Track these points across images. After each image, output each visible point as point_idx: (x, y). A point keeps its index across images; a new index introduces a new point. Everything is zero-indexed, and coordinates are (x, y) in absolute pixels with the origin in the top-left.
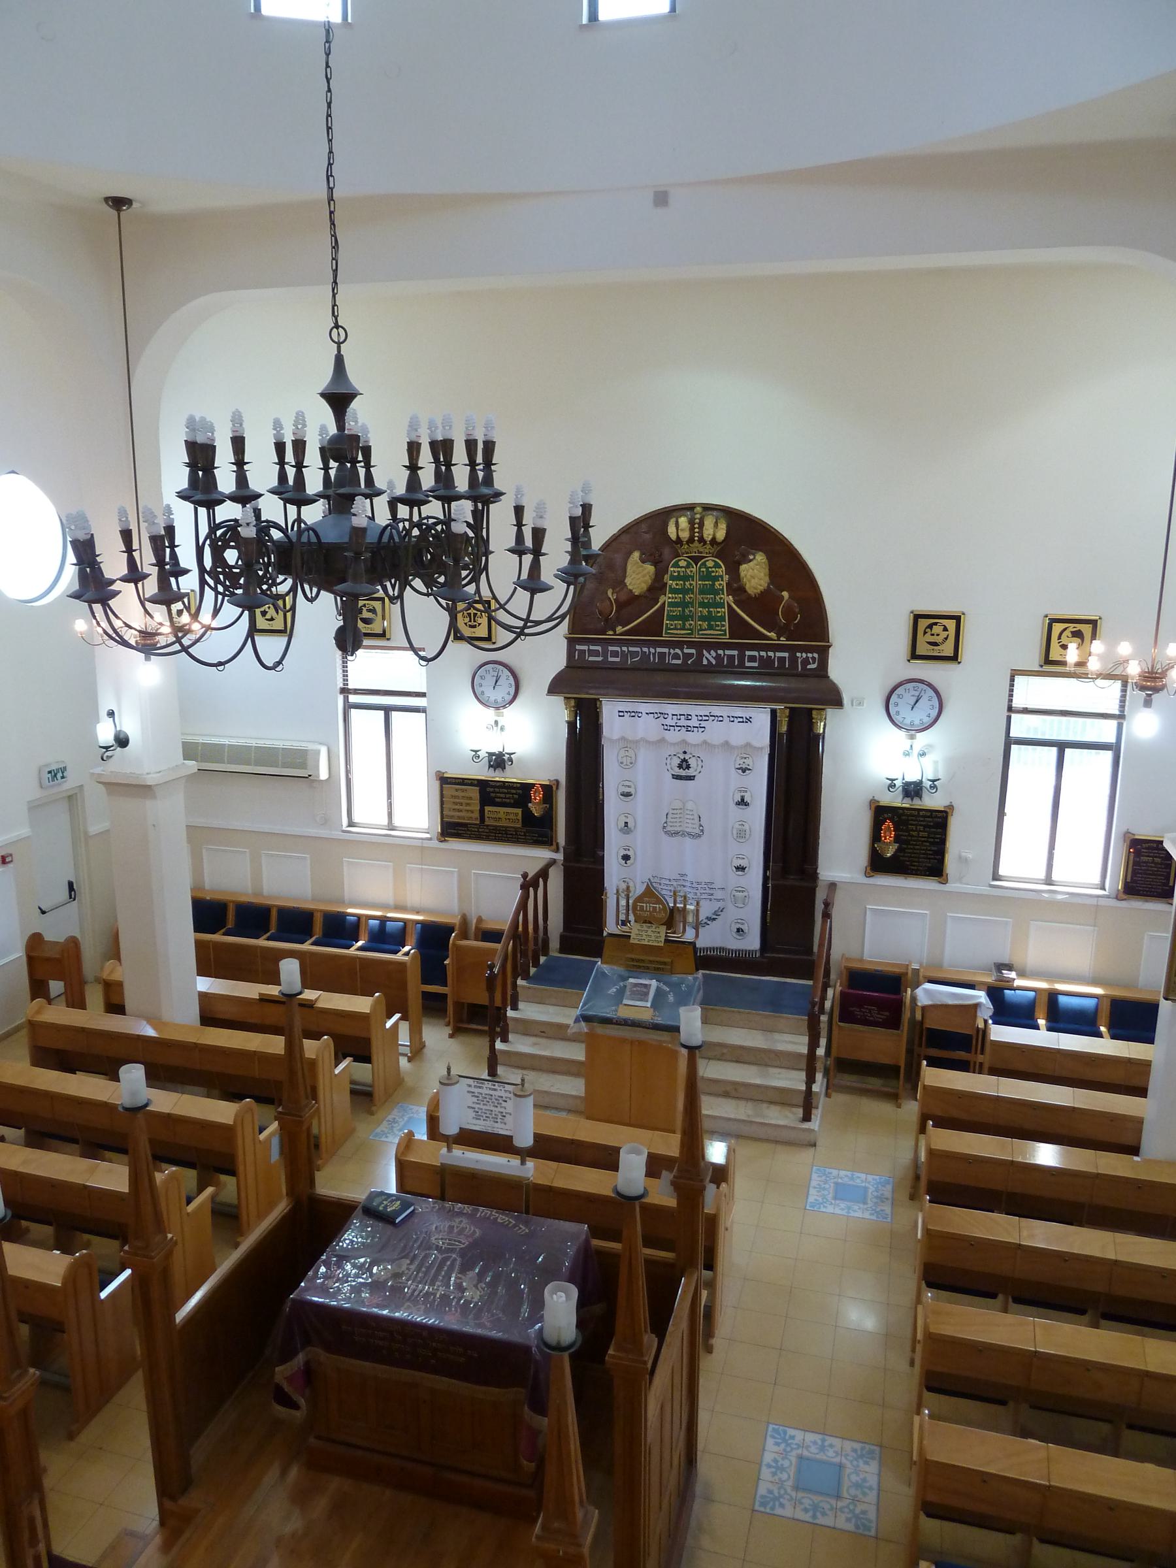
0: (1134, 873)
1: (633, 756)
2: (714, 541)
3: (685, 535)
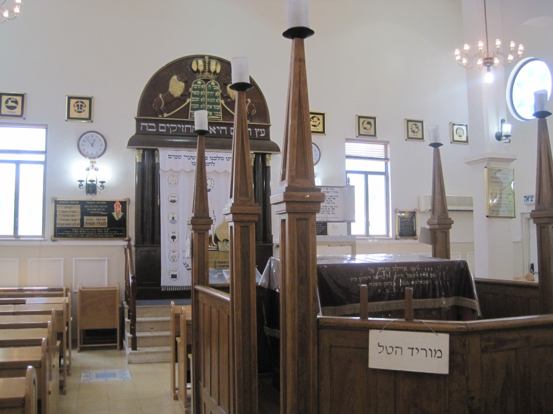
0: (401, 227)
1: (177, 180)
3: (201, 68)
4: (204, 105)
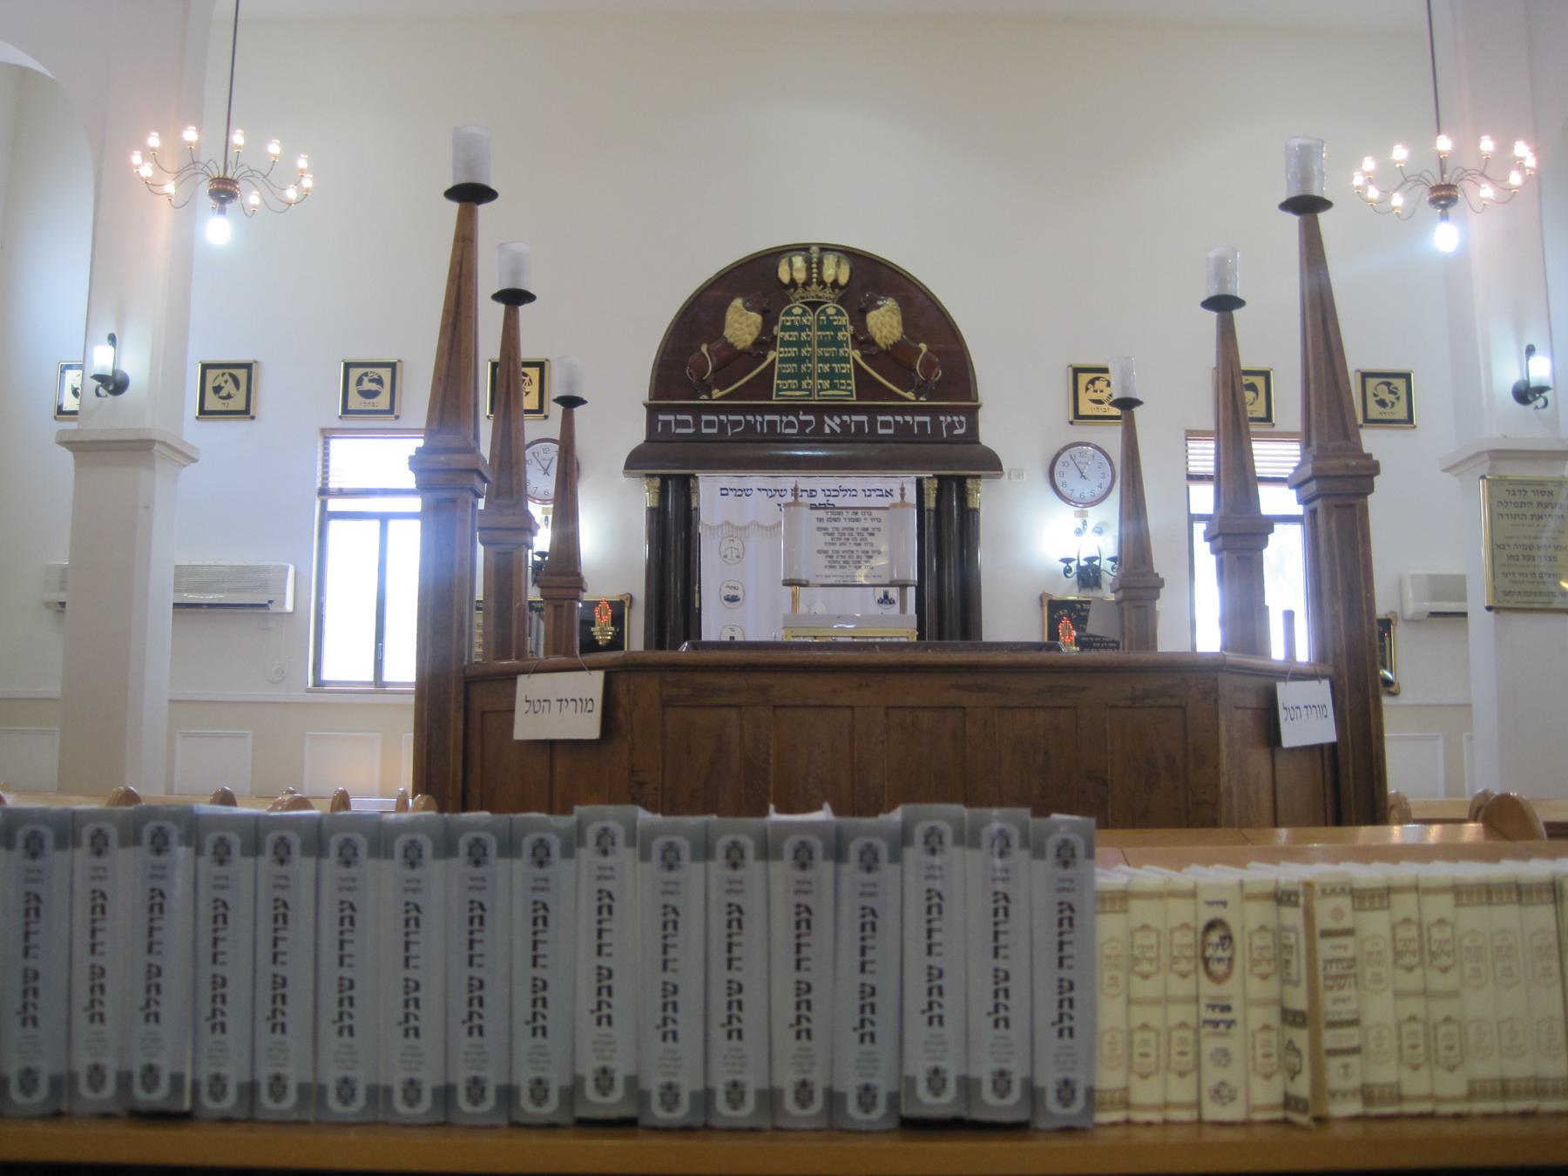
2: (835, 284)
3: (800, 276)
4: (810, 365)
